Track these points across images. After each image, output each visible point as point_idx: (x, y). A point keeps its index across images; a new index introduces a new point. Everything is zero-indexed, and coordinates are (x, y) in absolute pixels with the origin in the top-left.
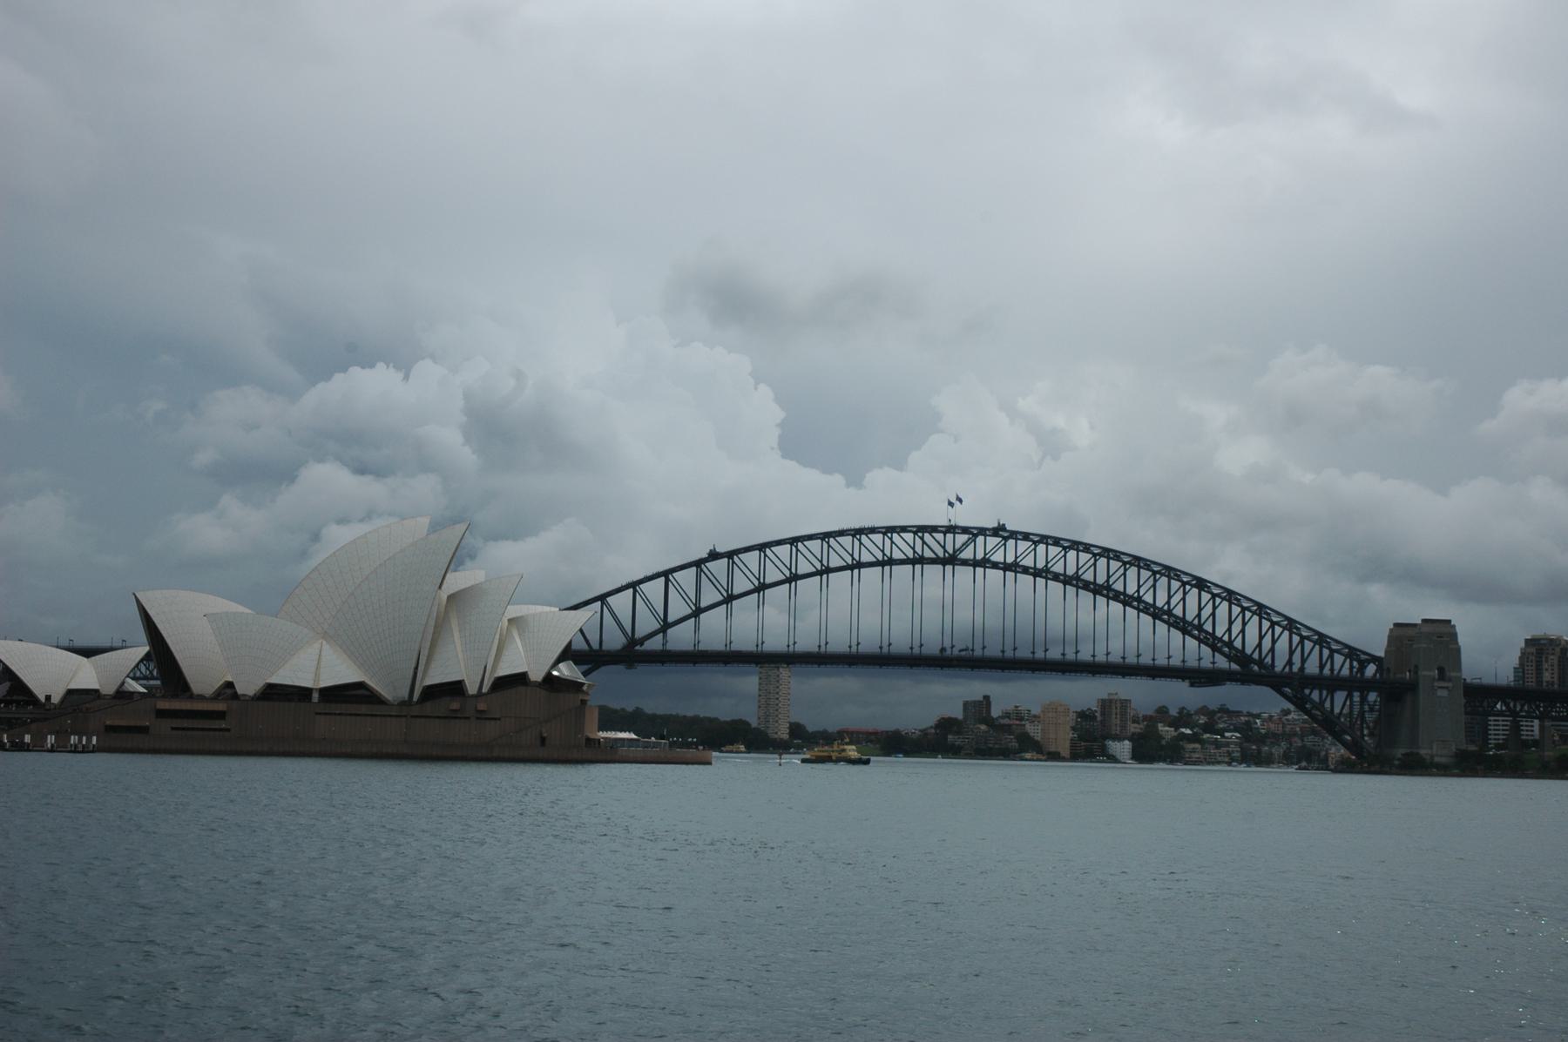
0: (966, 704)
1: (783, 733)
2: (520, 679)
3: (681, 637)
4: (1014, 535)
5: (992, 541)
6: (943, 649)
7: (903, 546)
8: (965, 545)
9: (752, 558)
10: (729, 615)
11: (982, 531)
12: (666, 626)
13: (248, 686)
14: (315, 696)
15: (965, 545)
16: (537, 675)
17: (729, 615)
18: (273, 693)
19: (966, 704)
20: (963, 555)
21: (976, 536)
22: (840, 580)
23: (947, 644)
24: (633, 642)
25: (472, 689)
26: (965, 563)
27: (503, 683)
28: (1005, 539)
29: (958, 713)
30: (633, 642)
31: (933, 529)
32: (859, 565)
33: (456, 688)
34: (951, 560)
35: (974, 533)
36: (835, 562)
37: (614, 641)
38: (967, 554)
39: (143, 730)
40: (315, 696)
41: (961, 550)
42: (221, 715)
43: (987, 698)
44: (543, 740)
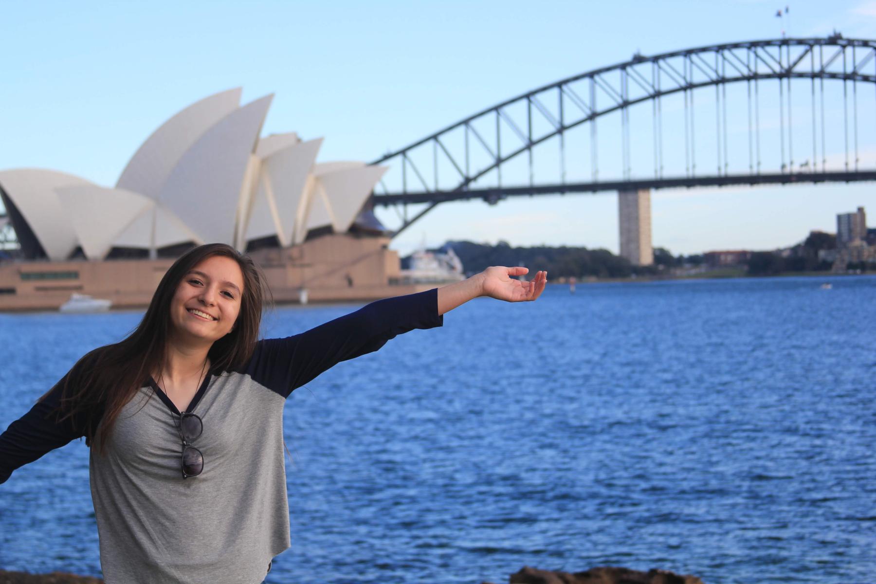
0: (839, 218)
1: (646, 259)
2: (327, 230)
3: (513, 174)
4: (851, 43)
5: (830, 51)
6: (783, 166)
7: (737, 63)
8: (801, 58)
9: (582, 87)
10: (562, 145)
11: (818, 42)
12: (499, 161)
13: (95, 248)
14: (153, 254)
15: (801, 58)
16: (342, 224)
17: (562, 145)
18: (117, 253)
19: (839, 218)
20: (799, 68)
21: (811, 46)
22: (673, 103)
23: (787, 161)
24: (468, 180)
25: (285, 240)
26: (801, 75)
27: (314, 234)
28: (844, 47)
29: (831, 228)
30: (468, 180)
31: (768, 43)
32: (690, 86)
33: (272, 242)
34: (786, 74)
35: (809, 44)
36: (666, 84)
37: (450, 181)
38: (804, 66)
39: (11, 291)
40: (153, 254)
41: (795, 64)
42: (75, 275)
43: (861, 210)
44: (350, 282)
